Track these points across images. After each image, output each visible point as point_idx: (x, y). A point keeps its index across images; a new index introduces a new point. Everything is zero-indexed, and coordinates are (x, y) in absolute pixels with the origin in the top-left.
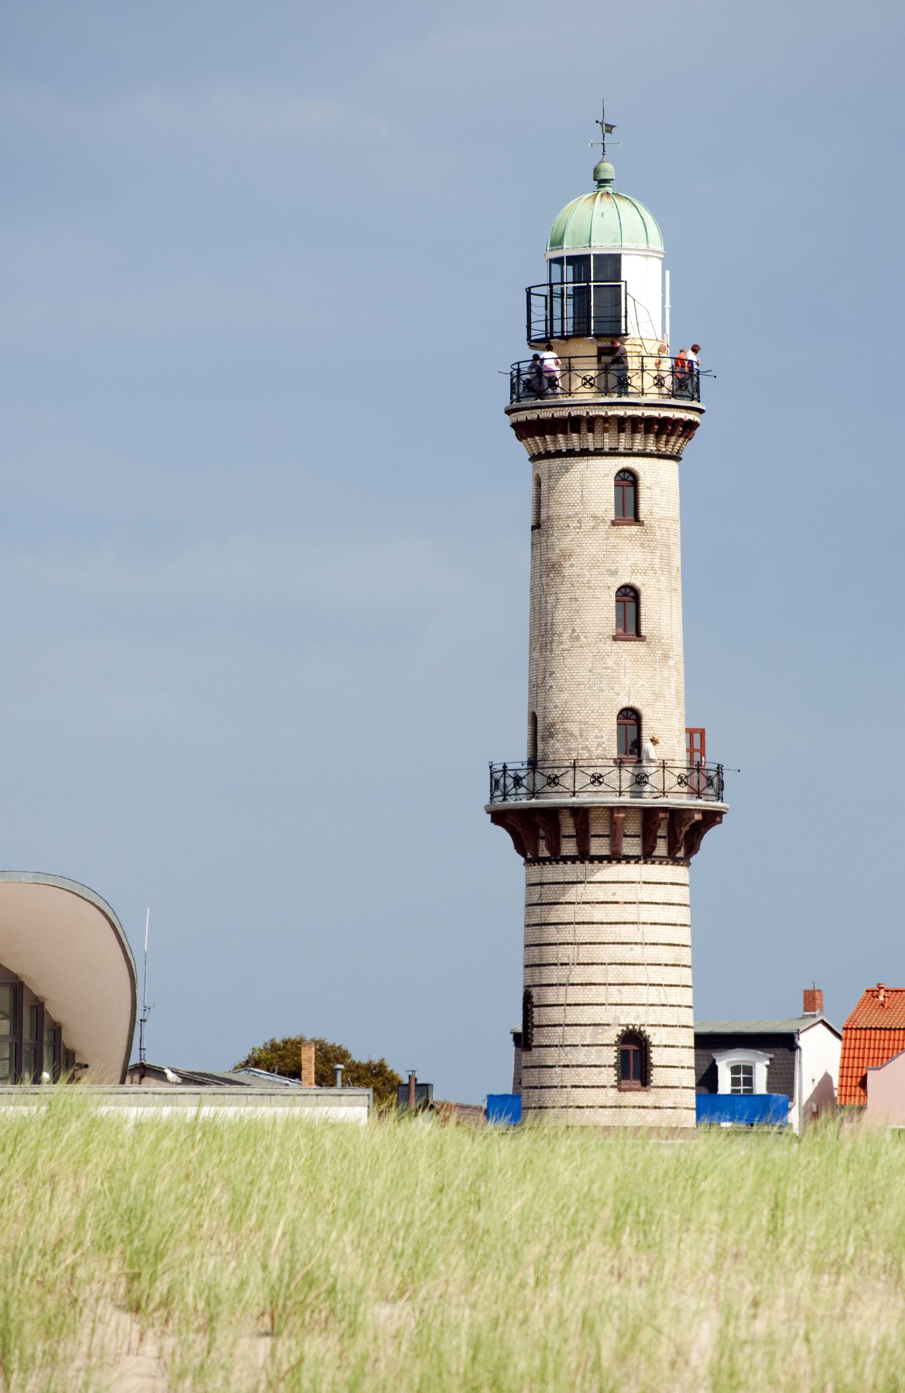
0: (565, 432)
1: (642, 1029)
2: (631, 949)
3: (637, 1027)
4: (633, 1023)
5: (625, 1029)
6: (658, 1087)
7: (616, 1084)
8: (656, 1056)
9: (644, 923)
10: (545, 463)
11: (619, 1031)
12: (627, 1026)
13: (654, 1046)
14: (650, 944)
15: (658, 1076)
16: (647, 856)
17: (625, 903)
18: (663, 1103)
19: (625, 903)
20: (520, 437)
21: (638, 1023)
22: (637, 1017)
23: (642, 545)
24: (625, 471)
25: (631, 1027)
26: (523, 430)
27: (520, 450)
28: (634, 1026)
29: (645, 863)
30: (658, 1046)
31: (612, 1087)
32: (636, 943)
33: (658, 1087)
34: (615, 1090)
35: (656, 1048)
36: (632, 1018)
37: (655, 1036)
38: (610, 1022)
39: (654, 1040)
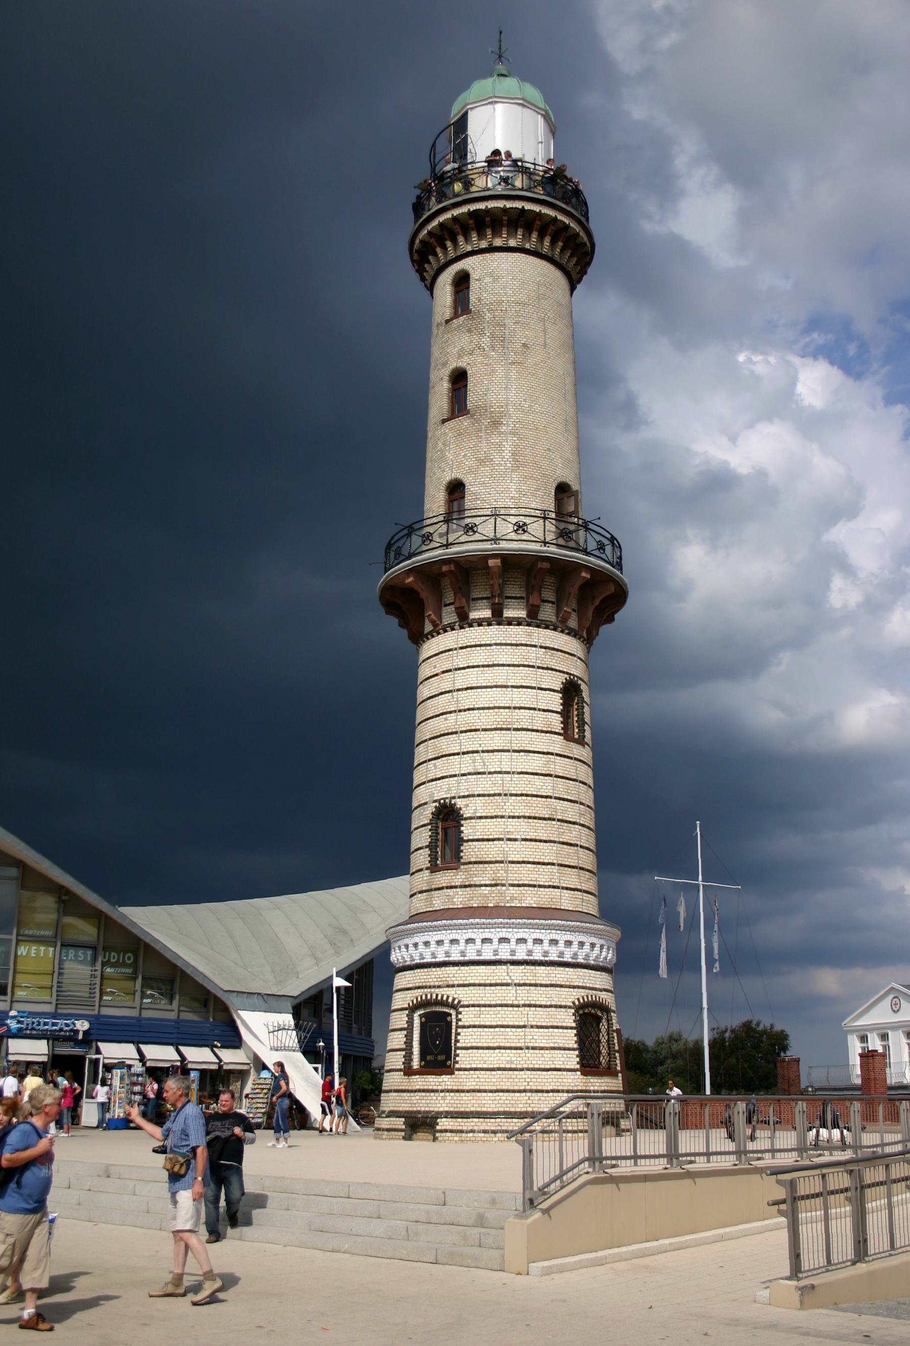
6: (470, 863)
8: (468, 830)
9: (458, 690)
16: (464, 621)
18: (476, 880)
21: (448, 796)
23: (469, 331)
24: (457, 273)
29: (462, 628)
30: (471, 818)
35: (468, 821)
37: (467, 808)
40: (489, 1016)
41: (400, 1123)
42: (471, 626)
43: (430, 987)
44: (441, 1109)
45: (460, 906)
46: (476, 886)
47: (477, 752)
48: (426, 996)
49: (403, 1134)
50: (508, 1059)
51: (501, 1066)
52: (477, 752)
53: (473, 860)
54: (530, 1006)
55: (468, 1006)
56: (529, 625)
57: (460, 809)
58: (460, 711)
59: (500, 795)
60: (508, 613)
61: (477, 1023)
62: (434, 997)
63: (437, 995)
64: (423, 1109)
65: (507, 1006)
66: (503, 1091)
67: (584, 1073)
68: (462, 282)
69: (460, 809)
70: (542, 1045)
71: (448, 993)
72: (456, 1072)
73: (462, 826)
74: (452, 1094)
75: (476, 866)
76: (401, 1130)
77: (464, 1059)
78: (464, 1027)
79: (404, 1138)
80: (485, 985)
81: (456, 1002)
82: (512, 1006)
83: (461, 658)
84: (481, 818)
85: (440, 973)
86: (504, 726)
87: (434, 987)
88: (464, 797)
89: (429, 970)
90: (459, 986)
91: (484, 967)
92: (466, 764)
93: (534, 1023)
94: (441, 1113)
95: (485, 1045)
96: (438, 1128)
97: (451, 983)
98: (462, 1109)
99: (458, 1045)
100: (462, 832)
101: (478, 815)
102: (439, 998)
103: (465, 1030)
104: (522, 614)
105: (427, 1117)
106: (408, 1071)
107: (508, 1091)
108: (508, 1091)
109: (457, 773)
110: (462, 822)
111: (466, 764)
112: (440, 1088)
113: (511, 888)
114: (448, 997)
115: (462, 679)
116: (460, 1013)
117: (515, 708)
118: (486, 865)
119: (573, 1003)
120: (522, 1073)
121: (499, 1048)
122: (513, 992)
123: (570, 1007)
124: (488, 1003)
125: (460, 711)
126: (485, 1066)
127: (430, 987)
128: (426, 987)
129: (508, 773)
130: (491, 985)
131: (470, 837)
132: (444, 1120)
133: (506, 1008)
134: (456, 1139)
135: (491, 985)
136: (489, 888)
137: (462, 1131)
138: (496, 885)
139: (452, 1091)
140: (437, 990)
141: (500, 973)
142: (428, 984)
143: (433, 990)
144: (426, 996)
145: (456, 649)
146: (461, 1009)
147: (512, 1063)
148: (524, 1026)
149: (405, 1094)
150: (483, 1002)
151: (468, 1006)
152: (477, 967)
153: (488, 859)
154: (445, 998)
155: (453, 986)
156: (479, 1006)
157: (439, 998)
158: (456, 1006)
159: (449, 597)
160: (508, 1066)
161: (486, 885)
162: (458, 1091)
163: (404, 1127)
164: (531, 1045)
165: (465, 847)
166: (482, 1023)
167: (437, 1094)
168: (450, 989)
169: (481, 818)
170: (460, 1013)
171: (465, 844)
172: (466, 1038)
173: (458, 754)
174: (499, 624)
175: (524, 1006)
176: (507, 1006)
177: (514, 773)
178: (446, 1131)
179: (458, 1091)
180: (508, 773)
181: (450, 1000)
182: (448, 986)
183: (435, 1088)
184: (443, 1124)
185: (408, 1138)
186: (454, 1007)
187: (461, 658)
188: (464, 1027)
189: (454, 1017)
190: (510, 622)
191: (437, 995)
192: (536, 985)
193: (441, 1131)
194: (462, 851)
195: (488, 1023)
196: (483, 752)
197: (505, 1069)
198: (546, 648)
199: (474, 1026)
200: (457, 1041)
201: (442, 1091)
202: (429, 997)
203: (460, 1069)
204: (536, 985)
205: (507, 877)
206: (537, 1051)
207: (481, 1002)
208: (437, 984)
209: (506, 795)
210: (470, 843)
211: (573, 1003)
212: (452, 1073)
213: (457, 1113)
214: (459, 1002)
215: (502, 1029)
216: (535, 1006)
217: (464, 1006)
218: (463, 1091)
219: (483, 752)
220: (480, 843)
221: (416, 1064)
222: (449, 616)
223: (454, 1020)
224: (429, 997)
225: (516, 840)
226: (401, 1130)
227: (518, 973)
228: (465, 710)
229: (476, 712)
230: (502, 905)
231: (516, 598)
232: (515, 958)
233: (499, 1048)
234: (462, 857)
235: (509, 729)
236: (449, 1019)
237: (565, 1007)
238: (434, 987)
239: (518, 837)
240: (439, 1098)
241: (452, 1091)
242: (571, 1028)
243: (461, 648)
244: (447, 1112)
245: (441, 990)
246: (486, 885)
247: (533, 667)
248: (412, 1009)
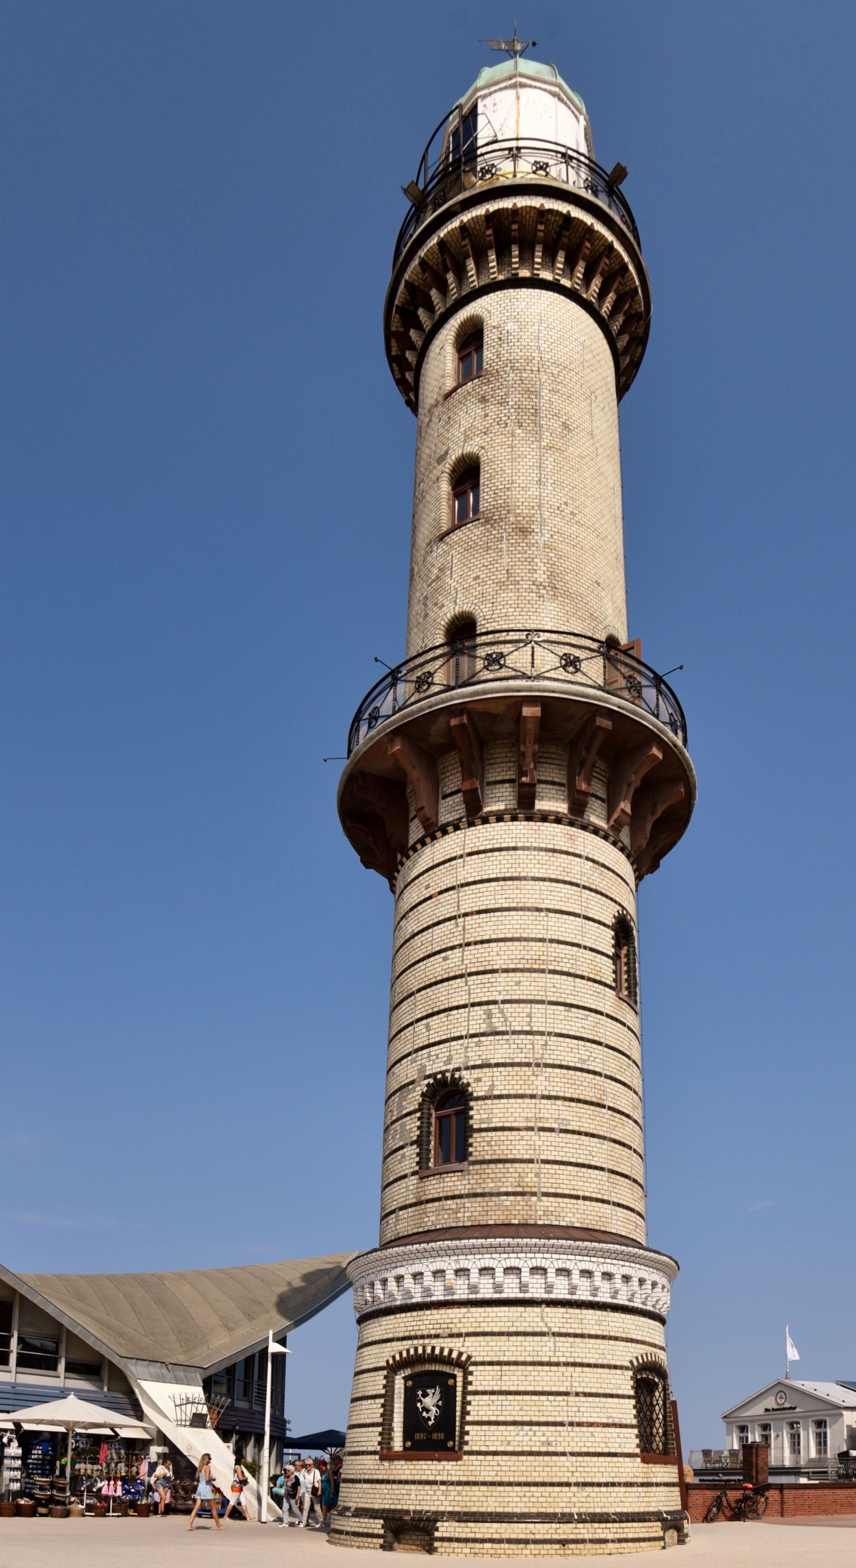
1: (457, 1076)
2: (445, 959)
3: (448, 1075)
4: (444, 1068)
5: (431, 1081)
6: (483, 1162)
7: (417, 1168)
8: (479, 1114)
9: (466, 915)
11: (422, 1086)
12: (433, 1076)
13: (478, 1099)
14: (476, 943)
15: (479, 1146)
16: (475, 814)
17: (441, 893)
19: (441, 893)
21: (450, 1067)
22: (449, 1060)
24: (463, 325)
25: (439, 1076)
28: (443, 1073)
29: (471, 824)
31: (414, 1174)
32: (452, 948)
33: (483, 1162)
34: (414, 1179)
35: (480, 1102)
36: (437, 1062)
37: (478, 1083)
38: (415, 1077)
39: (478, 1090)
40: (514, 1379)
41: (376, 1526)
42: (485, 821)
43: (423, 1337)
44: (442, 1509)
45: (469, 1224)
46: (491, 1195)
47: (494, 1002)
48: (416, 1349)
49: (381, 1541)
50: (544, 1439)
51: (534, 1449)
52: (494, 1002)
53: (488, 1157)
54: (574, 1364)
55: (483, 1363)
56: (571, 824)
57: (468, 1084)
58: (468, 944)
59: (528, 1065)
60: (541, 805)
61: (496, 1388)
62: (429, 1350)
63: (433, 1348)
64: (412, 1508)
65: (541, 1364)
66: (536, 1484)
67: (645, 1461)
68: (471, 339)
69: (468, 1084)
70: (591, 1420)
71: (451, 1345)
72: (465, 1457)
73: (472, 1109)
74: (459, 1488)
75: (493, 1166)
76: (378, 1536)
77: (475, 1438)
78: (476, 1393)
79: (382, 1547)
80: (509, 1334)
81: (464, 1358)
82: (549, 1364)
83: (472, 869)
84: (500, 1097)
85: (436, 1317)
86: (536, 966)
87: (429, 1336)
88: (474, 1067)
89: (420, 1313)
90: (469, 1334)
91: (506, 1309)
92: (476, 1020)
93: (580, 1390)
94: (443, 1513)
95: (509, 1419)
96: (437, 1534)
97: (455, 1331)
98: (474, 1509)
99: (468, 1418)
100: (471, 1117)
101: (496, 1093)
102: (437, 1352)
103: (477, 1397)
104: (562, 807)
105: (421, 1520)
106: (386, 1454)
107: (543, 1484)
108: (543, 1484)
109: (464, 1033)
110: (472, 1103)
111: (476, 1020)
112: (439, 1478)
113: (544, 1199)
114: (451, 1351)
115: (470, 899)
116: (471, 1373)
117: (552, 941)
118: (508, 1165)
119: (631, 1362)
120: (563, 1458)
121: (530, 1423)
122: (550, 1344)
123: (627, 1368)
124: (513, 1359)
125: (468, 944)
126: (509, 1449)
127: (423, 1337)
128: (416, 1337)
129: (542, 1033)
130: (517, 1334)
131: (484, 1126)
132: (446, 1524)
133: (540, 1368)
134: (467, 1551)
135: (517, 1334)
136: (511, 1198)
137: (475, 1540)
138: (522, 1194)
139: (459, 1483)
140: (434, 1342)
141: (531, 1318)
142: (419, 1333)
143: (427, 1341)
144: (416, 1349)
145: (461, 856)
146: (471, 1368)
147: (549, 1444)
148: (567, 1394)
149: (383, 1486)
150: (506, 1359)
151: (483, 1363)
152: (496, 1309)
153: (510, 1157)
154: (446, 1353)
155: (459, 1335)
156: (499, 1363)
157: (437, 1352)
158: (464, 1364)
159: (453, 781)
160: (544, 1449)
161: (507, 1194)
162: (467, 1483)
163: (382, 1532)
164: (577, 1420)
166: (504, 1388)
167: (435, 1487)
168: (454, 1340)
169: (500, 1097)
170: (471, 1373)
171: (475, 1135)
172: (479, 1408)
173: (465, 1006)
174: (529, 819)
175: (567, 1364)
176: (541, 1364)
177: (549, 1034)
178: (450, 1540)
179: (467, 1483)
180: (542, 1033)
181: (454, 1355)
182: (451, 1336)
183: (431, 1478)
184: (445, 1529)
185: (387, 1547)
187: (472, 869)
188: (476, 1393)
189: (460, 1379)
190: (544, 817)
191: (433, 1348)
192: (582, 1336)
193: (442, 1539)
194: (471, 1145)
195: (513, 1388)
196: (504, 1002)
197: (539, 1454)
198: (594, 861)
199: (493, 1393)
200: (465, 1413)
201: (443, 1483)
202: (420, 1351)
203: (471, 1453)
204: (582, 1336)
205: (539, 1182)
206: (584, 1429)
207: (502, 1359)
208: (433, 1332)
209: (538, 1065)
210: (484, 1134)
211: (631, 1362)
212: (459, 1458)
213: (466, 1514)
214: (469, 1357)
215: (534, 1398)
216: (582, 1365)
217: (476, 1364)
218: (475, 1484)
219: (504, 1002)
220: (499, 1133)
221: (398, 1444)
222: (450, 809)
223: (459, 1384)
224: (420, 1351)
225: (551, 1130)
226: (378, 1536)
227: (556, 1318)
228: (476, 943)
229: (492, 945)
230: (532, 1222)
231: (553, 783)
232: (552, 1296)
233: (530, 1423)
234: (471, 1154)
235: (543, 971)
236: (451, 1382)
237: (621, 1368)
238: (429, 1336)
239: (555, 1126)
240: (438, 1493)
241: (459, 1483)
242: (629, 1397)
243: (470, 854)
244: (450, 1513)
245: (440, 1340)
246: (507, 1194)
247: (577, 885)
248: (393, 1368)
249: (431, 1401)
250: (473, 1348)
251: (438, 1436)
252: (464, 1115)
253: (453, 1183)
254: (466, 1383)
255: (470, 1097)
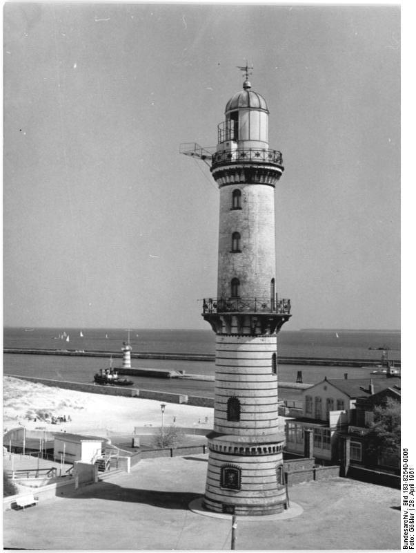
0: (234, 175)
8: (243, 408)
10: (223, 188)
13: (242, 405)
15: (243, 416)
20: (216, 179)
26: (217, 176)
27: (216, 184)
37: (242, 401)
40: (251, 473)
165: (241, 414)
172: (244, 480)
186: (238, 469)
249: (232, 476)
250: (242, 466)
251: (234, 485)
252: (239, 408)
253: (237, 424)
254: (241, 474)
255: (240, 404)
